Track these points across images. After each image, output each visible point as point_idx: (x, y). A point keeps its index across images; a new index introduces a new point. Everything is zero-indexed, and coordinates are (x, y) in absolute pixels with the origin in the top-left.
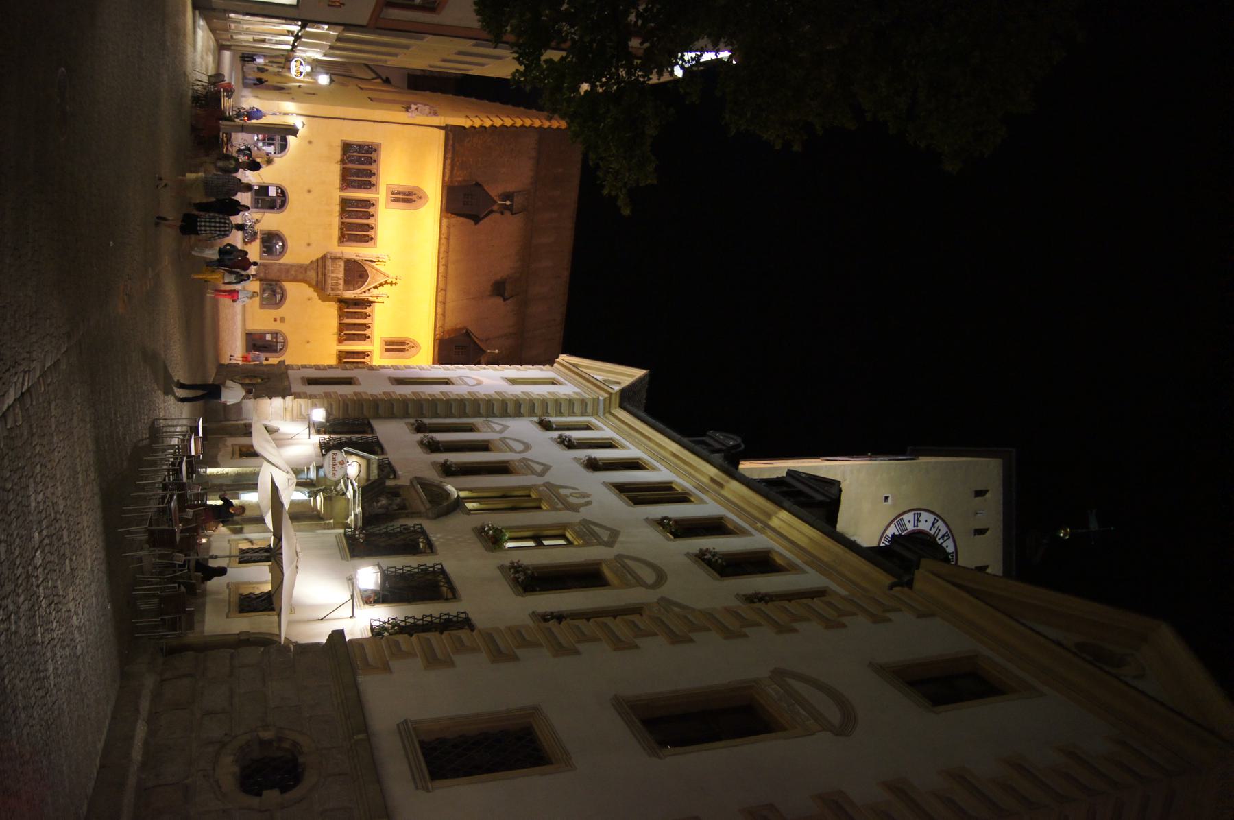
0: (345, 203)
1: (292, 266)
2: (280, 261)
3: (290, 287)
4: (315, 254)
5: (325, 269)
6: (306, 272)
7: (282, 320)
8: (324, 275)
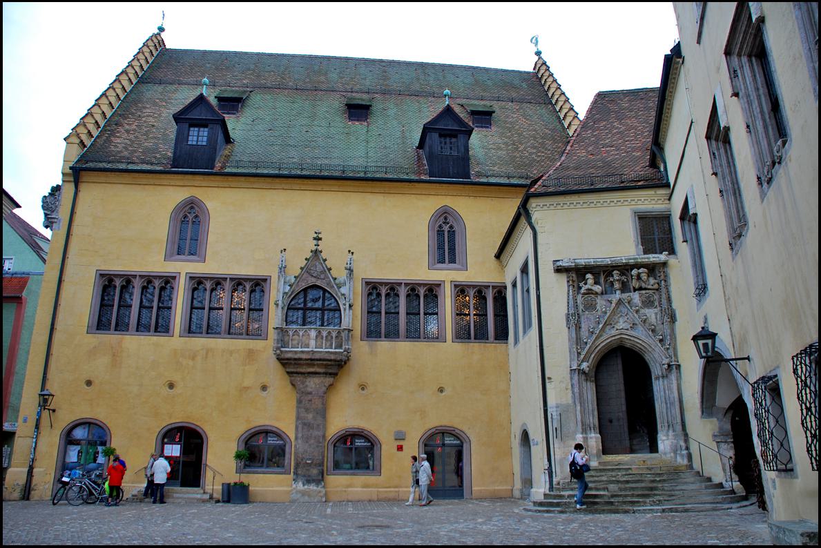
0: (191, 330)
1: (298, 418)
2: (292, 437)
3: (341, 419)
4: (275, 375)
5: (300, 359)
6: (310, 393)
7: (400, 436)
8: (311, 361)
